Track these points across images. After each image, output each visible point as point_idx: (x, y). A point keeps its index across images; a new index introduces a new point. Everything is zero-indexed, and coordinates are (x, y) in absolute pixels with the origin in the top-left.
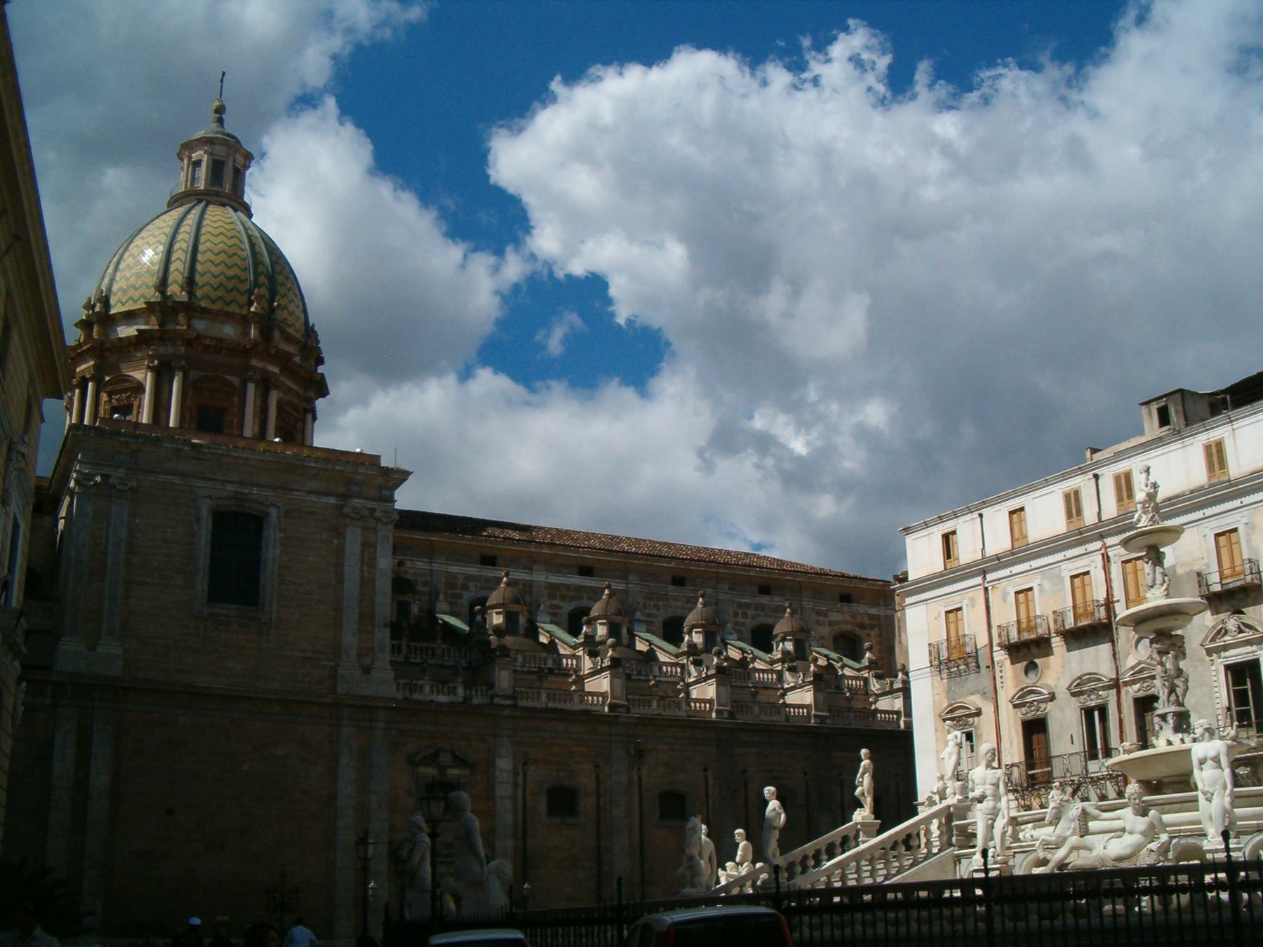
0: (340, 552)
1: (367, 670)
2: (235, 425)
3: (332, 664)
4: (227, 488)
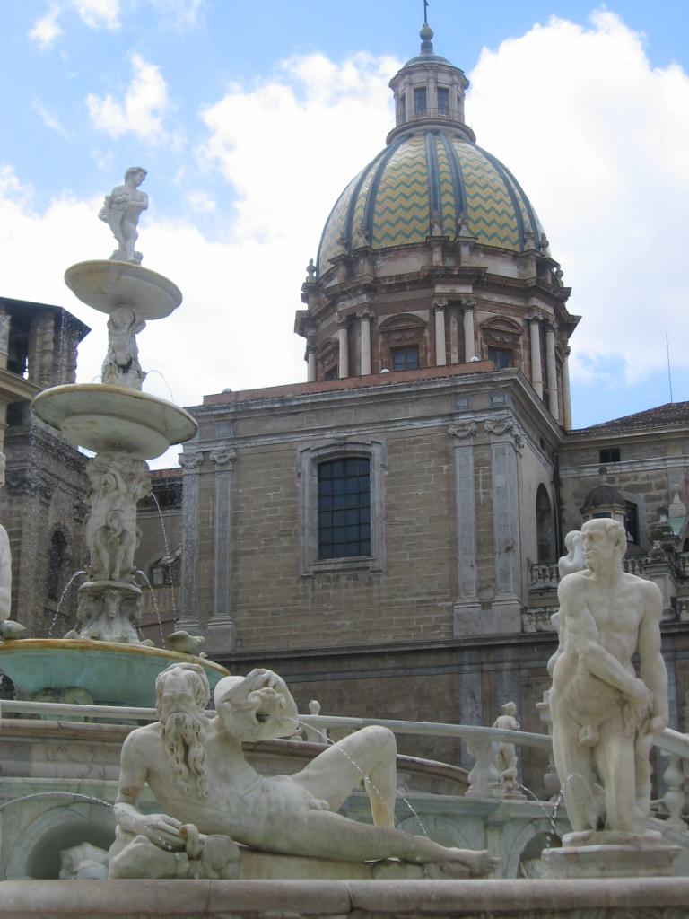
0: (450, 478)
1: (486, 605)
2: (428, 359)
3: (450, 603)
4: (326, 436)
